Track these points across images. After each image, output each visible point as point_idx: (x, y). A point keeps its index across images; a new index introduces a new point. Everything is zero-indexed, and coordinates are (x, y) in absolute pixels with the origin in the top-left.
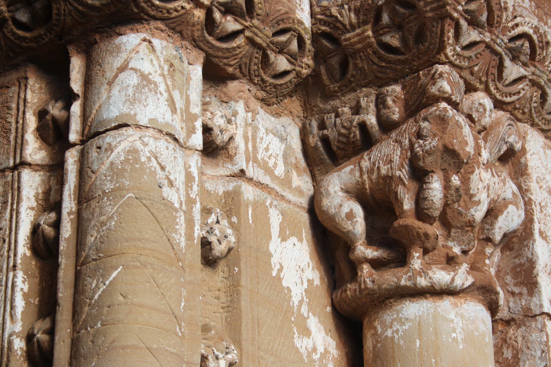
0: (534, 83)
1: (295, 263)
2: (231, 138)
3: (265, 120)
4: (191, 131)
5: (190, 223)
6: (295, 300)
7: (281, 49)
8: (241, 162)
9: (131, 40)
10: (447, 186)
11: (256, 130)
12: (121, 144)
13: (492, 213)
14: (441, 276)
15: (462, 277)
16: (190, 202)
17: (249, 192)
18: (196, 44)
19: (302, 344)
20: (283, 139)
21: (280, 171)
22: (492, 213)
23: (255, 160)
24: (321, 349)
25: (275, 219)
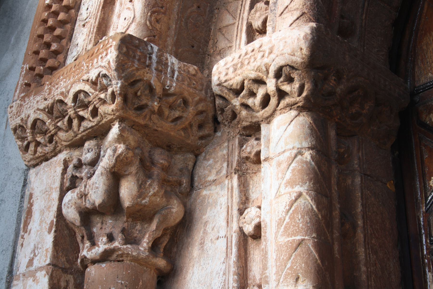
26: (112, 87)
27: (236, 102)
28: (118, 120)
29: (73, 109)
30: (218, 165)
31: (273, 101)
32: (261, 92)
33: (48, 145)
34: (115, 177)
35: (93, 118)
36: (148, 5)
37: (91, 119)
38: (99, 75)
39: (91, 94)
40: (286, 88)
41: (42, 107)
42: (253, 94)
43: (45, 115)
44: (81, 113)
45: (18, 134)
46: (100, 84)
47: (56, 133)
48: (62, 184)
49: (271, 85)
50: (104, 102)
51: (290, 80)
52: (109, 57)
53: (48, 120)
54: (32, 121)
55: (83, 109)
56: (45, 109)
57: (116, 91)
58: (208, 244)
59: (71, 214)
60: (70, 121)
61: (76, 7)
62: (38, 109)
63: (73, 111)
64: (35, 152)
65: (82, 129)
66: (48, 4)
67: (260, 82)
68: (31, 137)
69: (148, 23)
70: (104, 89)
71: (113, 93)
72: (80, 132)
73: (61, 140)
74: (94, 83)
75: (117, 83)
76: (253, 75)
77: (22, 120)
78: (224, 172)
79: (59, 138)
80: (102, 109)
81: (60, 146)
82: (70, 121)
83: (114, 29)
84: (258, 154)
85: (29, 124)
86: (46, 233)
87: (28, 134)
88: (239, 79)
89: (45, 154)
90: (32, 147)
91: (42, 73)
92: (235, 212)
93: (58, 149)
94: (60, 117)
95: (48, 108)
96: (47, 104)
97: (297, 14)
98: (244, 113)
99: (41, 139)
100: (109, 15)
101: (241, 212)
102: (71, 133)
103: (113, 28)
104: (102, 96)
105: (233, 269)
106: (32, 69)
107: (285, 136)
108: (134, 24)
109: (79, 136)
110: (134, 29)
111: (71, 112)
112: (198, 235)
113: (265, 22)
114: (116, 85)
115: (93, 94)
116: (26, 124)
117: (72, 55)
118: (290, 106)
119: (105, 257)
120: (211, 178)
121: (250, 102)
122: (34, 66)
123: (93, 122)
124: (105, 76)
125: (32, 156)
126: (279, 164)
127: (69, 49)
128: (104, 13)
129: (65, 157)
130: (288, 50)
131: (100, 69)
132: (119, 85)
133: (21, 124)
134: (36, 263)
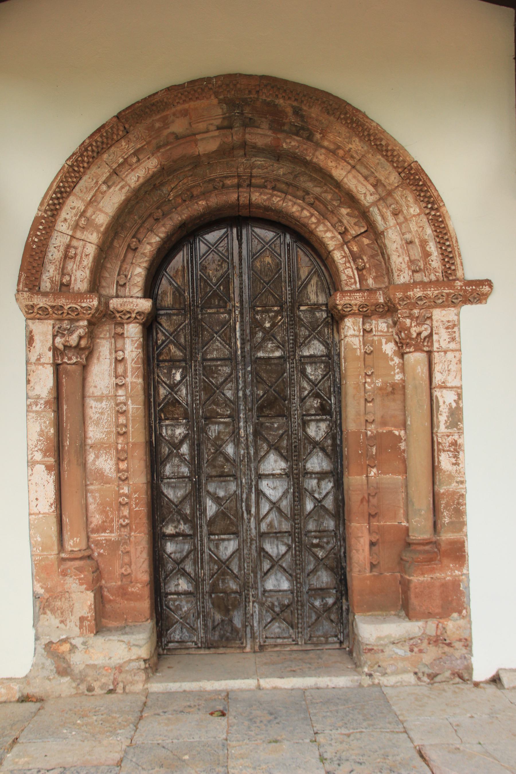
0: (430, 302)
1: (389, 348)
2: (372, 329)
3: (380, 321)
4: (360, 332)
5: (360, 350)
6: (390, 355)
7: (380, 307)
8: (374, 333)
9: (346, 320)
10: (405, 333)
11: (378, 324)
12: (347, 339)
13: (419, 334)
14: (408, 350)
15: (412, 349)
16: (360, 346)
17: (376, 338)
18: (360, 315)
19: (391, 363)
20: (386, 323)
21: (386, 330)
22: (419, 334)
23: (378, 331)
24: (397, 362)
25: (384, 341)
27: (118, 315)
30: (105, 333)
31: (132, 319)
32: (129, 315)
34: (81, 338)
40: (138, 317)
41: (49, 304)
42: (124, 314)
48: (53, 333)
49: (133, 315)
50: (84, 313)
51: (140, 315)
52: (94, 303)
58: (101, 359)
59: (61, 347)
60: (63, 313)
67: (129, 312)
70: (87, 310)
74: (82, 307)
76: (128, 310)
78: (108, 336)
82: (63, 313)
84: (123, 334)
85: (38, 307)
86: (47, 351)
88: (122, 309)
90: (35, 314)
92: (113, 352)
97: (140, 288)
98: (119, 319)
101: (116, 352)
105: (113, 370)
107: (133, 331)
112: (96, 355)
113: (125, 284)
114: (93, 311)
116: (36, 305)
118: (137, 323)
119: (74, 364)
120: (102, 336)
121: (123, 317)
126: (132, 341)
130: (143, 308)
134: (42, 360)
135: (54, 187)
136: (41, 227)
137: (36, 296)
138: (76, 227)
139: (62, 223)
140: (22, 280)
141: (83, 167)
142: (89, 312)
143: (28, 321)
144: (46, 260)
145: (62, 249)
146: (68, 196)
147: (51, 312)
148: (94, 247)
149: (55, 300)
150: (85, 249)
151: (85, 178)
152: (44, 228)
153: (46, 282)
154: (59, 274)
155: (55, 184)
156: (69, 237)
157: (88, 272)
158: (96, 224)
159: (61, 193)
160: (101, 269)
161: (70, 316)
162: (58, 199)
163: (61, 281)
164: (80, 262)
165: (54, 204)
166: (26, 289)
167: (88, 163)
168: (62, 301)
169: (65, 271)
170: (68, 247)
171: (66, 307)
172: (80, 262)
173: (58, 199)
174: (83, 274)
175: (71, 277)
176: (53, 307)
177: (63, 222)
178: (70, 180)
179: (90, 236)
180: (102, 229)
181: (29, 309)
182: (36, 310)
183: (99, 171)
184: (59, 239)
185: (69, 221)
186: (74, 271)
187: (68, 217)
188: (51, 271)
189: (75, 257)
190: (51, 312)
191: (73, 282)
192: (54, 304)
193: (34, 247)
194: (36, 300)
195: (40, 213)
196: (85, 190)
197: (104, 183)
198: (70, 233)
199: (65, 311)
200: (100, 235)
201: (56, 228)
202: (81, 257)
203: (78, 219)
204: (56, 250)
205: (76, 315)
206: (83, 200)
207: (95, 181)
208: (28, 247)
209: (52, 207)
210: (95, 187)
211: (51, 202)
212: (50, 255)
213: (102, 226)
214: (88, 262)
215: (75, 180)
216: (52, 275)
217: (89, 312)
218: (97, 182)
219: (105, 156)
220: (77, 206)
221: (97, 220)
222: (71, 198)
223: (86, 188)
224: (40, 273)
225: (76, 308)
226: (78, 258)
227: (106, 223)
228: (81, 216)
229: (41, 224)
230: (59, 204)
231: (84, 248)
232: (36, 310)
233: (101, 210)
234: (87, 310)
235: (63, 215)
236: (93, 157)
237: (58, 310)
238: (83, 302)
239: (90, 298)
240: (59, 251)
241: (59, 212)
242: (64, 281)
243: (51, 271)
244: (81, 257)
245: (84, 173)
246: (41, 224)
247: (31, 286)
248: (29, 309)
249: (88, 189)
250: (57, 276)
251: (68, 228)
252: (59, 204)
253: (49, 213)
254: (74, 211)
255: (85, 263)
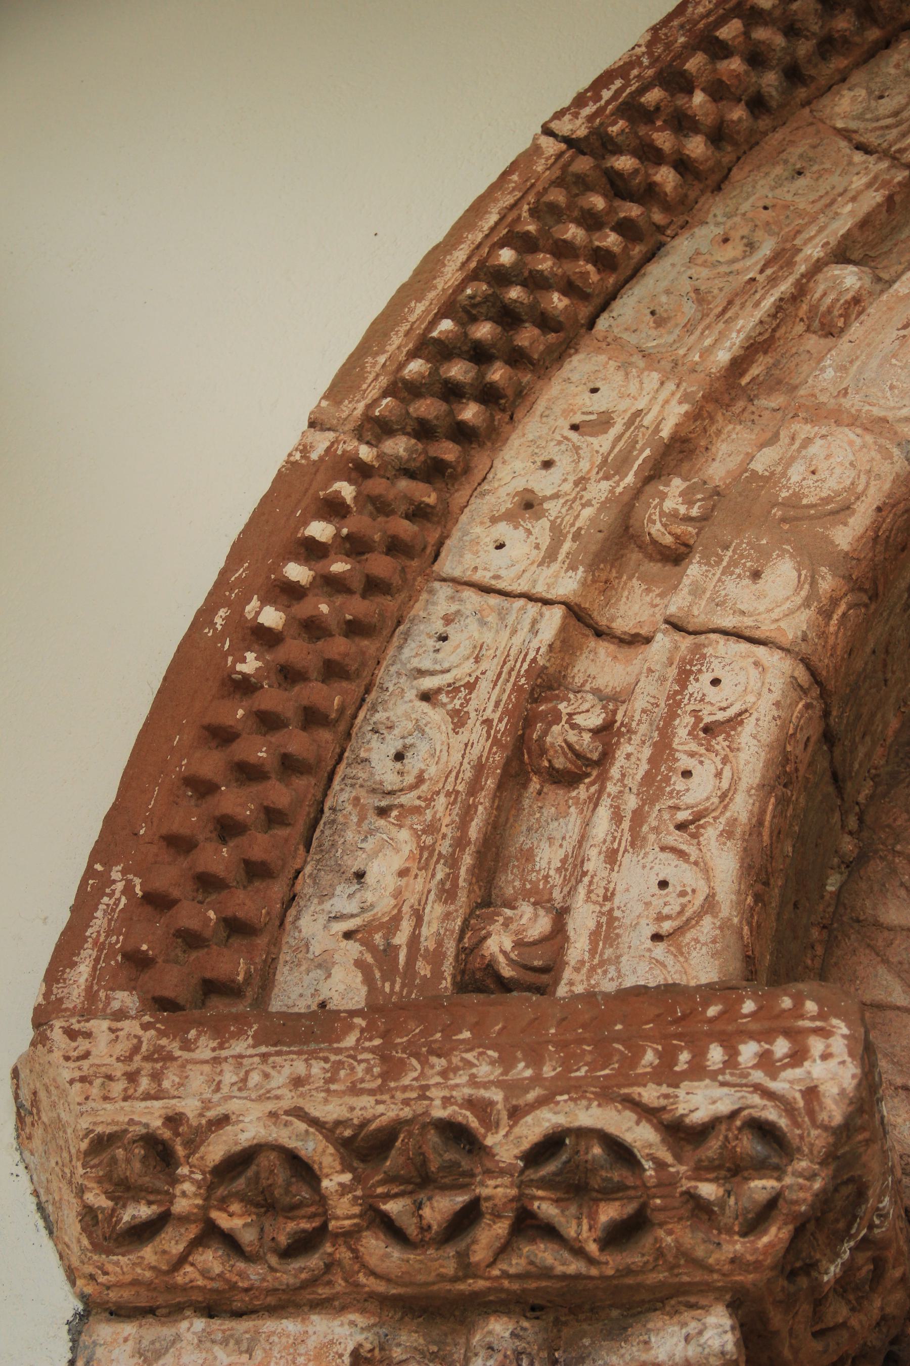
26: (779, 1179)
28: (728, 1297)
29: (517, 1181)
33: (273, 1260)
35: (602, 1250)
36: (750, 867)
37: (592, 1248)
38: (734, 1114)
39: (647, 1165)
41: (330, 1110)
43: (331, 1150)
44: (546, 1208)
45: (114, 1161)
46: (723, 1147)
47: (350, 1236)
53: (342, 1172)
54: (246, 1144)
55: (559, 1195)
56: (338, 1123)
57: (796, 1202)
60: (466, 1219)
61: (342, 727)
62: (298, 1113)
63: (513, 1192)
64: (182, 1260)
65: (516, 1264)
66: (246, 677)
68: (199, 1201)
69: (746, 929)
70: (733, 1170)
71: (772, 1203)
72: (496, 1272)
73: (364, 1266)
74: (680, 1133)
75: (812, 1177)
77: (174, 1120)
79: (357, 1257)
80: (673, 1235)
81: (340, 1285)
82: (466, 1219)
83: (593, 896)
85: (216, 1150)
87: (187, 1187)
89: (233, 1287)
90: (173, 1242)
91: (207, 933)
93: (323, 1292)
94: (408, 1181)
95: (365, 1123)
96: (368, 1114)
99: (245, 1225)
100: (507, 819)
102: (444, 1261)
103: (590, 892)
104: (708, 1190)
106: (157, 902)
108: (707, 921)
109: (481, 1284)
110: (714, 942)
111: (497, 1190)
114: (801, 1181)
115: (661, 1165)
116: (194, 1142)
117: (327, 906)
122: (176, 893)
123: (591, 1261)
124: (763, 1130)
125: (148, 1274)
127: (298, 872)
128: (499, 808)
129: (360, 1338)
131: (756, 1099)
132: (817, 1185)
133: (167, 1134)
135: (451, 273)
136: (320, 530)
137: (205, 1048)
138: (622, 545)
139: (503, 530)
140: (99, 922)
141: (682, 165)
142: (761, 1187)
143: (104, 1331)
144: (341, 795)
145: (488, 701)
146: (559, 355)
147: (344, 1211)
148: (779, 668)
149: (392, 1069)
150: (700, 686)
151: (683, 247)
152: (354, 546)
153: (325, 965)
154: (448, 893)
155: (460, 255)
156: (556, 615)
157: (725, 863)
158: (794, 502)
159: (509, 318)
160: (830, 944)
161: (545, 1254)
162: (480, 355)
163: (468, 951)
164: (653, 785)
165: (452, 392)
166: (124, 999)
167: (718, 136)
168: (461, 1079)
169: (510, 882)
170: (543, 687)
171: (507, 1144)
172: (653, 785)
173: (480, 355)
174: (682, 875)
175: (561, 916)
176: (365, 1147)
177: (510, 517)
178: (573, 232)
179: (738, 590)
180: (845, 536)
181: (123, 1190)
182: (186, 1198)
183: (801, 194)
184: (463, 637)
185: (553, 508)
186: (595, 862)
187: (545, 484)
188: (383, 870)
189: (607, 756)
190: (344, 1211)
191: (578, 947)
192: (385, 1111)
193: (250, 664)
194: (197, 1080)
195: (321, 442)
196: (689, 309)
197: (841, 254)
198: (567, 584)
199: (497, 1190)
200: (827, 583)
201: (448, 565)
202: (663, 749)
203: (637, 492)
204: (435, 716)
205: (620, 1235)
206: (675, 368)
207: (766, 249)
208: (194, 671)
209: (427, 408)
210: (773, 281)
211: (416, 367)
212: (379, 754)
213: (843, 510)
214: (730, 779)
215: (611, 240)
216: (384, 905)
217: (761, 1187)
218: (783, 258)
219: (846, 105)
220: (624, 408)
221: (796, 473)
222: (580, 366)
223: (700, 297)
224: (277, 890)
225: (620, 1152)
226: (632, 758)
227: (874, 496)
228: (656, 472)
229: (333, 509)
230: (489, 396)
231: (684, 677)
232: (186, 1198)
233: (817, 413)
234: (733, 1170)
235: (512, 469)
236: (757, 104)
237: (421, 1181)
238: (698, 1071)
239: (769, 1026)
240: (459, 719)
241: (480, 461)
242: (499, 944)
243: (383, 870)
244: (663, 749)
245: (683, 212)
246: (333, 509)
247: (172, 980)
248: (123, 1190)
249: (714, 309)
250: (434, 911)
251: (551, 556)
252: (489, 396)
253: (399, 446)
254: (603, 443)
255: (700, 789)
